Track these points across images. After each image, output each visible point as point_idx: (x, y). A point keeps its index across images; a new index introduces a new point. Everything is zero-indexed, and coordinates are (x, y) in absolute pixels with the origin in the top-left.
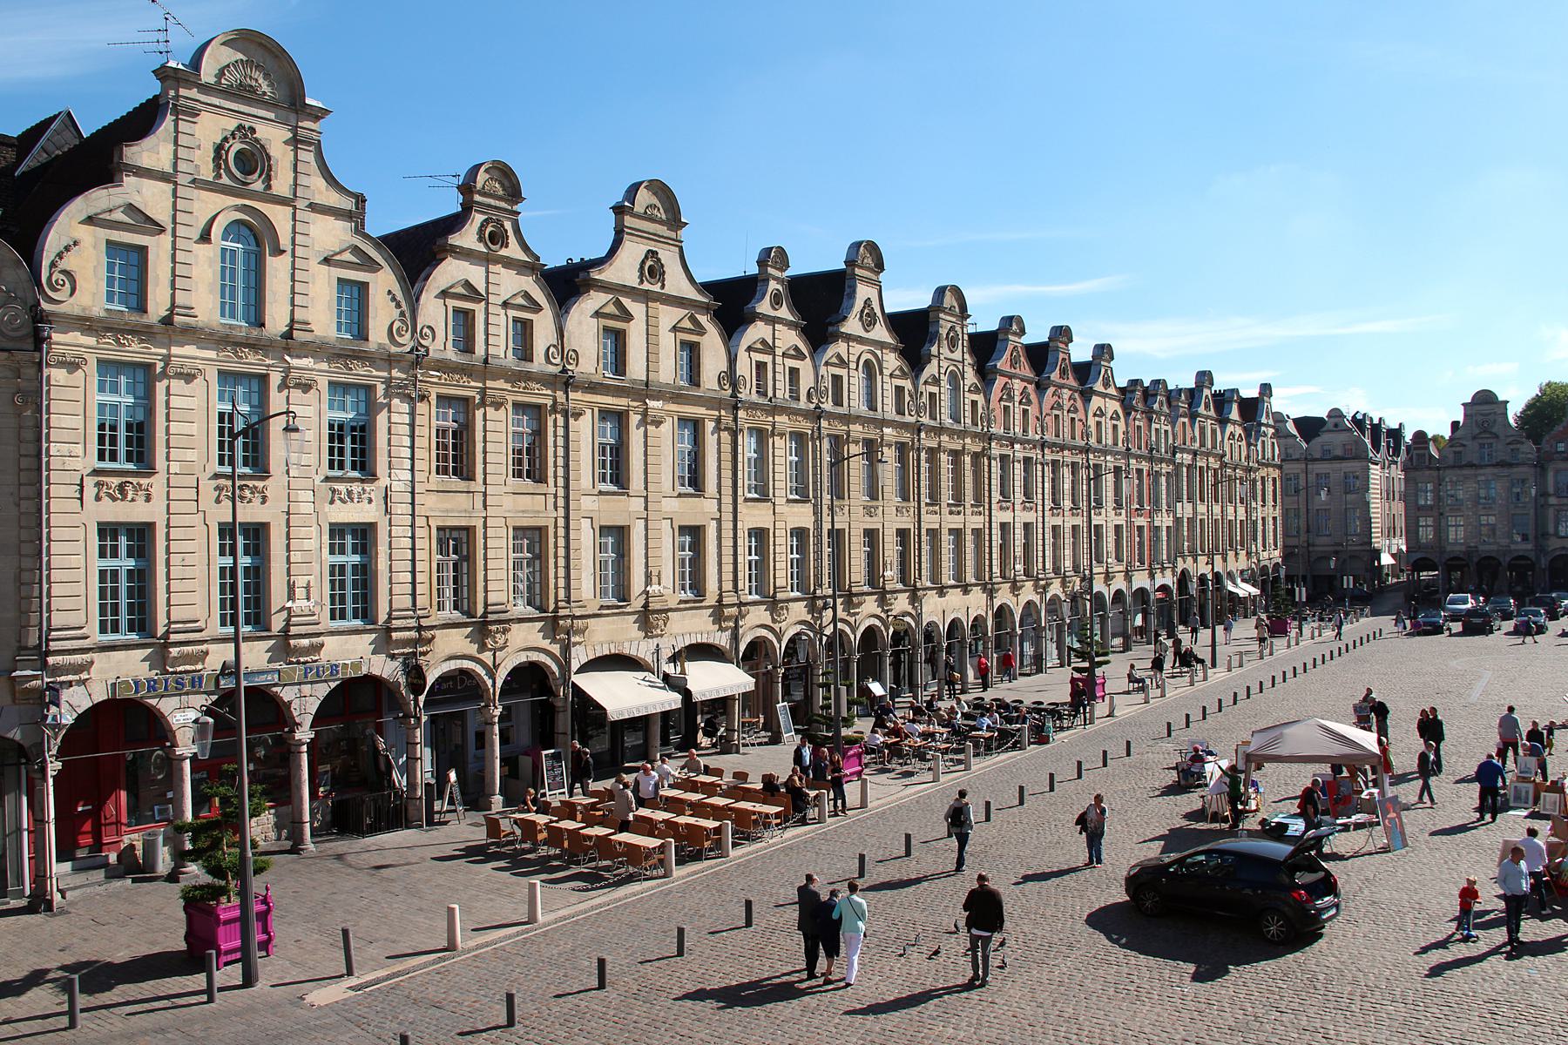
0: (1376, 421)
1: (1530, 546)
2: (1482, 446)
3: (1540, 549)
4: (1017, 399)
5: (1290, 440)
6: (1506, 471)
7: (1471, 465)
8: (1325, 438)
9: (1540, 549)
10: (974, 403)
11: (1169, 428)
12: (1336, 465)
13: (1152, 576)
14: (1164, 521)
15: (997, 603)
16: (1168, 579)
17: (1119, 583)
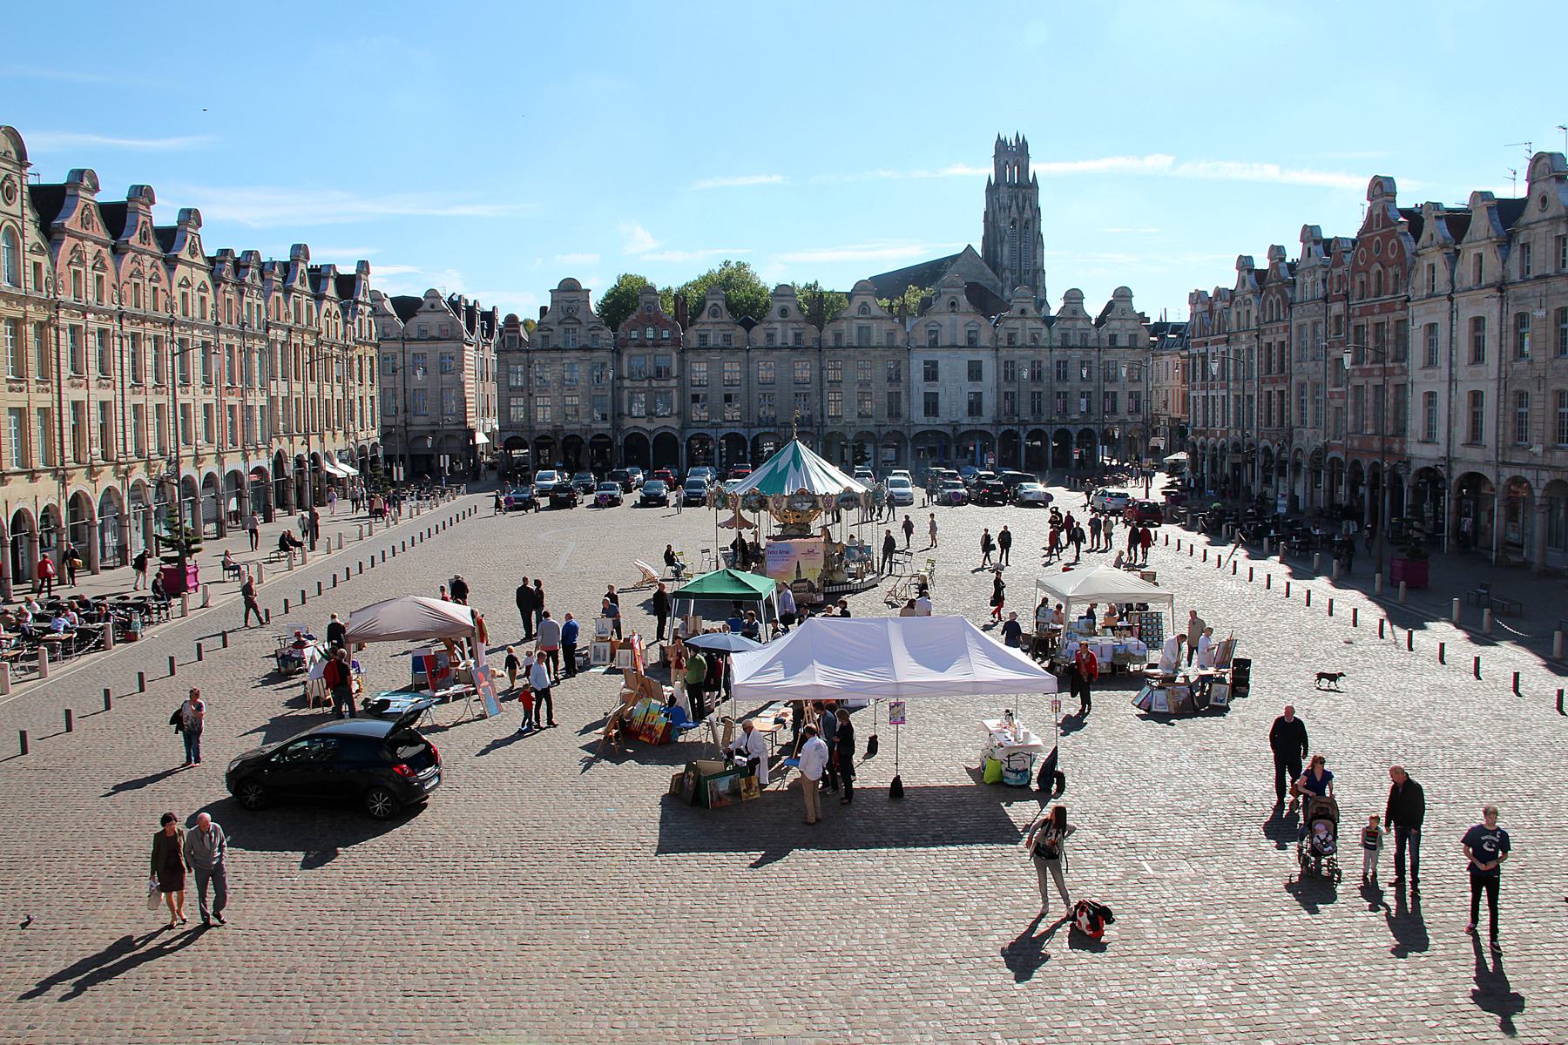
0: (471, 304)
1: (608, 426)
2: (567, 330)
3: (617, 428)
4: (90, 263)
5: (387, 319)
6: (588, 355)
7: (557, 349)
8: (421, 318)
9: (617, 428)
10: (37, 266)
11: (262, 302)
12: (433, 345)
13: (246, 458)
14: (258, 400)
15: (71, 491)
16: (264, 461)
17: (210, 466)
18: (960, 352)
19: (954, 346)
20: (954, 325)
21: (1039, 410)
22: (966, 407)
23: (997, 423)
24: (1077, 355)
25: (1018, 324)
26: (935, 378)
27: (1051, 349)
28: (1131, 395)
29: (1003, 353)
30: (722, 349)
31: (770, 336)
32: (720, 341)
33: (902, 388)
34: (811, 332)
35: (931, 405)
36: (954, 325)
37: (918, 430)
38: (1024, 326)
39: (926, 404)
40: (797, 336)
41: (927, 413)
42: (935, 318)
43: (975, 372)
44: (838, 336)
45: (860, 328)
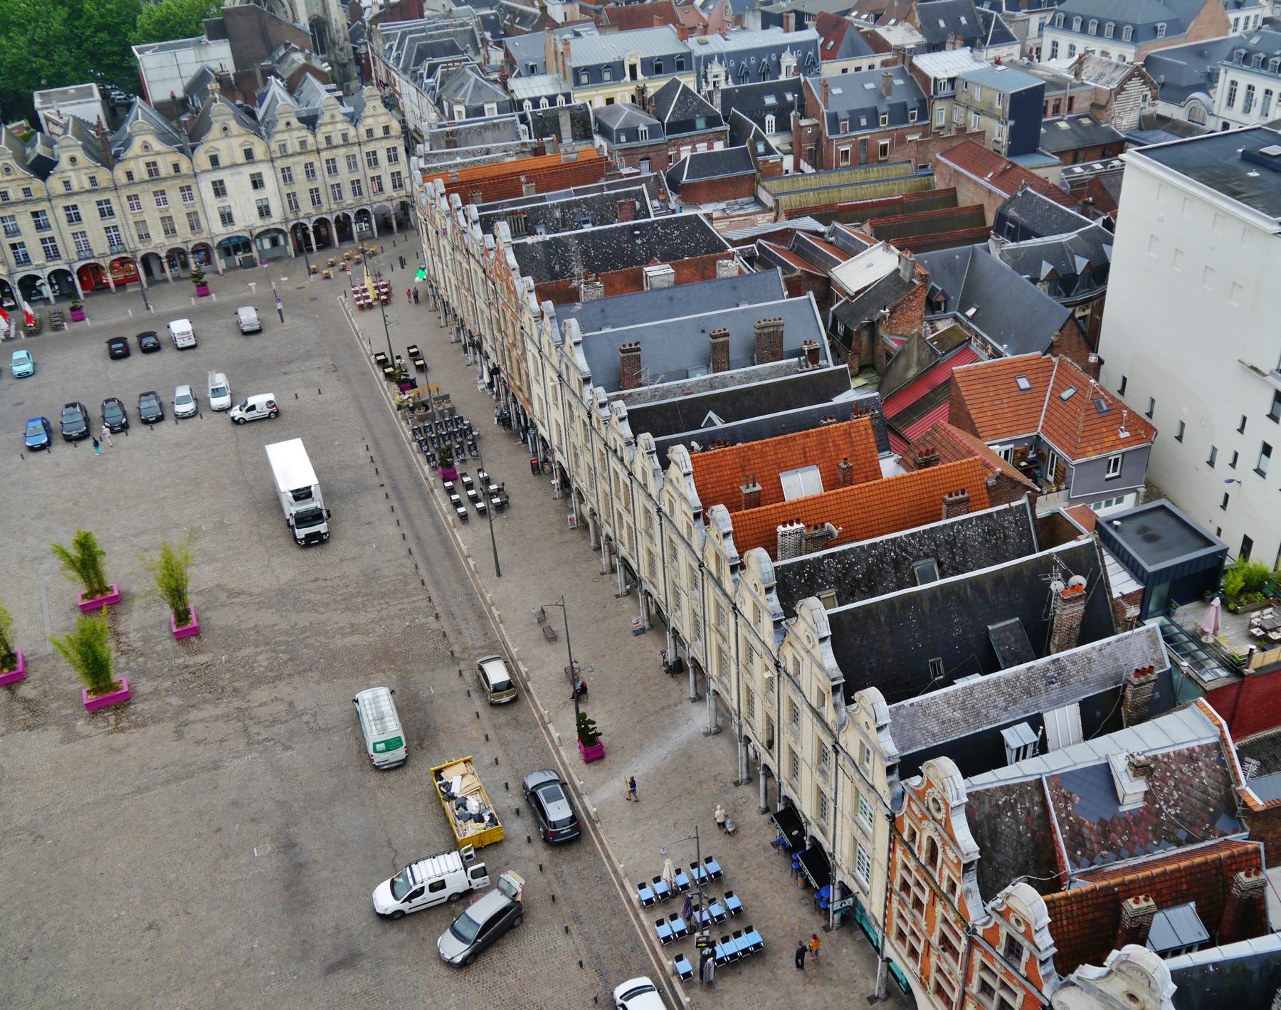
18: (242, 169)
19: (234, 165)
20: (230, 147)
21: (319, 202)
22: (256, 212)
23: (287, 221)
24: (342, 151)
25: (285, 136)
26: (224, 193)
27: (318, 151)
28: (393, 174)
29: (280, 164)
30: (24, 202)
31: (67, 184)
32: (21, 196)
33: (198, 208)
34: (103, 176)
35: (227, 218)
36: (230, 147)
37: (220, 239)
38: (291, 137)
39: (222, 216)
40: (93, 180)
41: (224, 222)
42: (214, 144)
43: (257, 183)
44: (130, 175)
45: (148, 165)
